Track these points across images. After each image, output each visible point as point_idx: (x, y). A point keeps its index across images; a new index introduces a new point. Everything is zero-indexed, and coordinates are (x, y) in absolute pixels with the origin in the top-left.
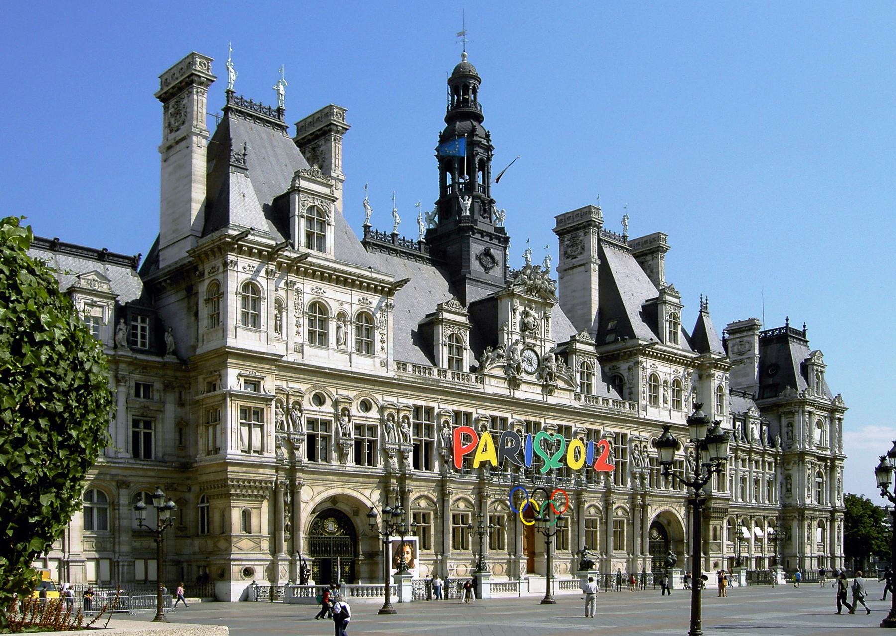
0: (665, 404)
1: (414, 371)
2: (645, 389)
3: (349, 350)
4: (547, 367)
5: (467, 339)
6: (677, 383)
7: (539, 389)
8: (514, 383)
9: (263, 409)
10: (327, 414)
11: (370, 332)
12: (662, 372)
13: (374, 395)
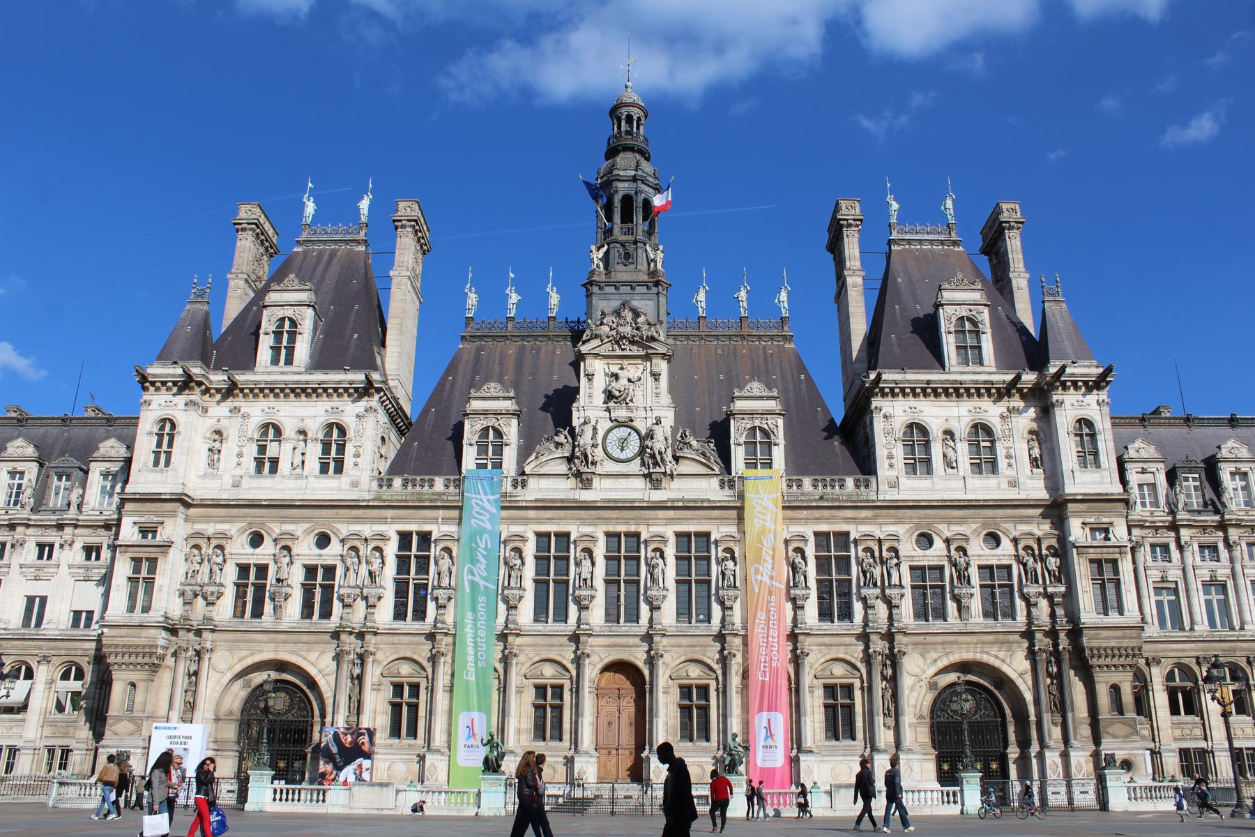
0: (949, 471)
1: (405, 485)
2: (894, 452)
3: (305, 474)
4: (647, 447)
5: (512, 430)
6: (981, 429)
7: (640, 483)
8: (584, 480)
9: (157, 558)
10: (264, 557)
11: (341, 448)
12: (936, 417)
13: (335, 525)
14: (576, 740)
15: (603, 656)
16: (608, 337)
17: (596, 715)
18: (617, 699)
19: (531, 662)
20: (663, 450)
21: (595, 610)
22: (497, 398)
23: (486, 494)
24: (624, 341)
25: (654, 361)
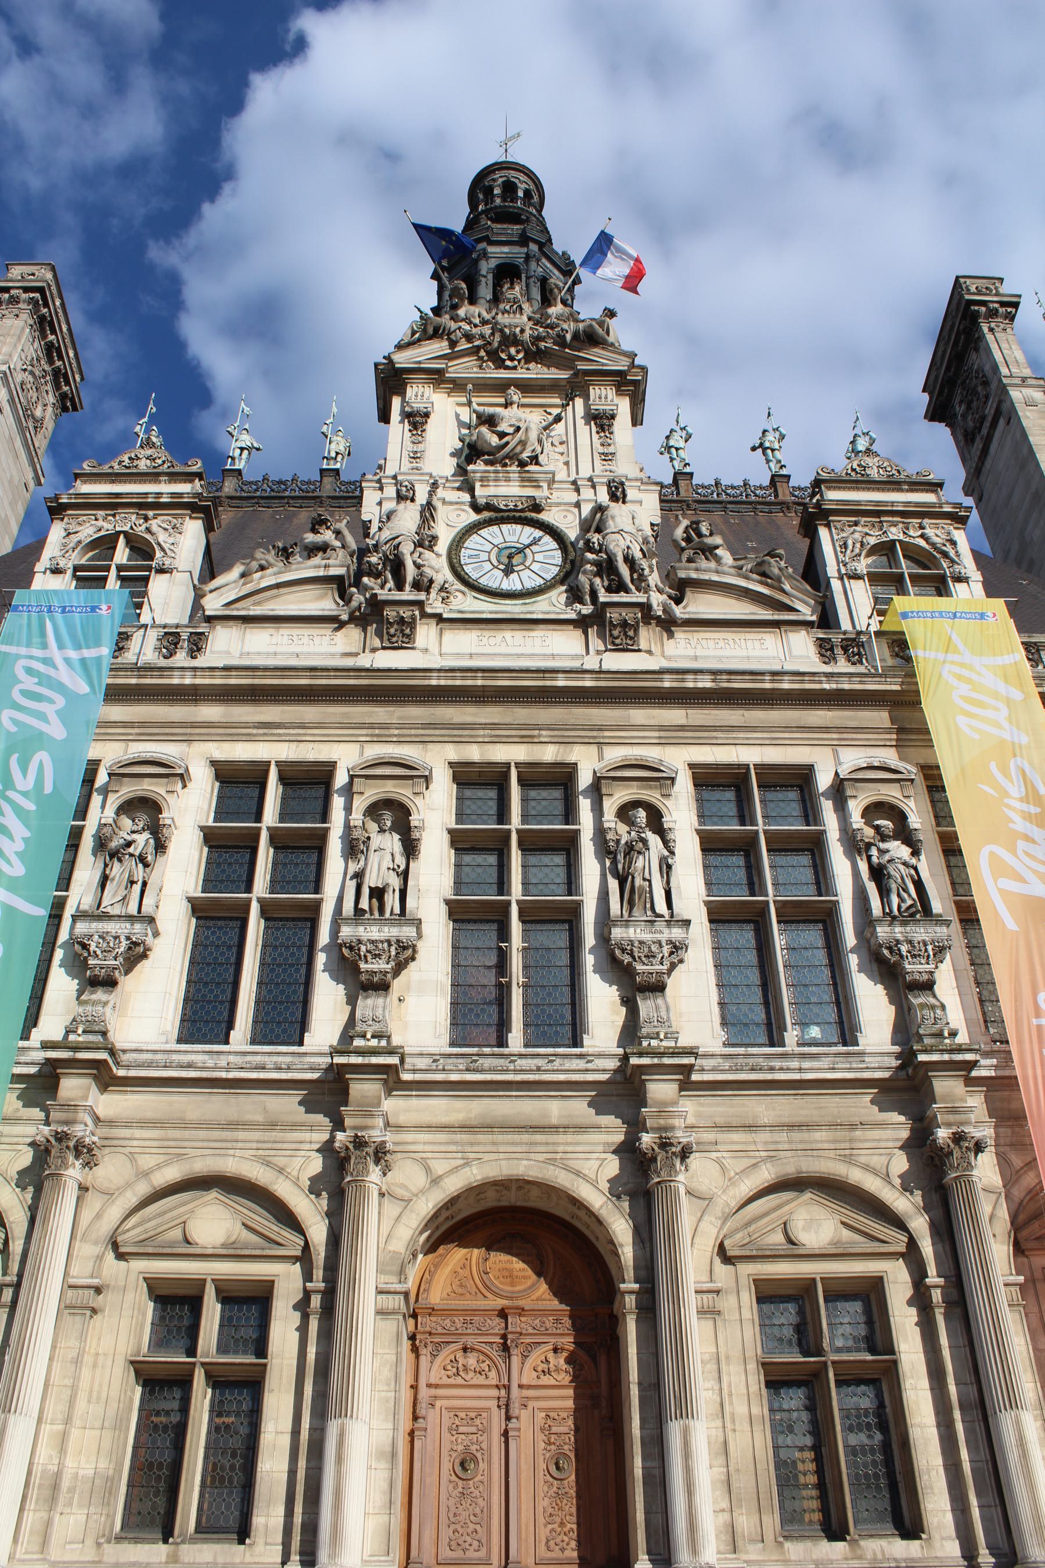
14: (311, 1529)
15: (440, 1167)
16: (469, 338)
17: (405, 1423)
18: (495, 1353)
19: (143, 1189)
20: (638, 555)
21: (411, 1000)
22: (153, 476)
23: (61, 646)
24: (513, 351)
25: (594, 392)
